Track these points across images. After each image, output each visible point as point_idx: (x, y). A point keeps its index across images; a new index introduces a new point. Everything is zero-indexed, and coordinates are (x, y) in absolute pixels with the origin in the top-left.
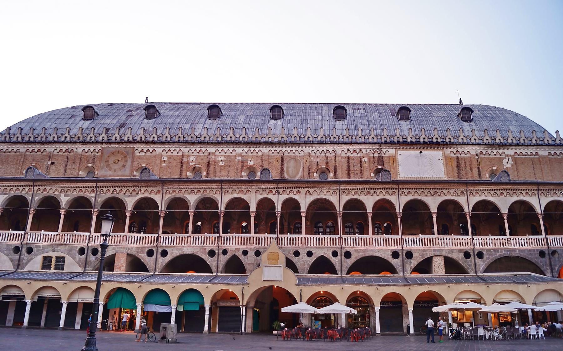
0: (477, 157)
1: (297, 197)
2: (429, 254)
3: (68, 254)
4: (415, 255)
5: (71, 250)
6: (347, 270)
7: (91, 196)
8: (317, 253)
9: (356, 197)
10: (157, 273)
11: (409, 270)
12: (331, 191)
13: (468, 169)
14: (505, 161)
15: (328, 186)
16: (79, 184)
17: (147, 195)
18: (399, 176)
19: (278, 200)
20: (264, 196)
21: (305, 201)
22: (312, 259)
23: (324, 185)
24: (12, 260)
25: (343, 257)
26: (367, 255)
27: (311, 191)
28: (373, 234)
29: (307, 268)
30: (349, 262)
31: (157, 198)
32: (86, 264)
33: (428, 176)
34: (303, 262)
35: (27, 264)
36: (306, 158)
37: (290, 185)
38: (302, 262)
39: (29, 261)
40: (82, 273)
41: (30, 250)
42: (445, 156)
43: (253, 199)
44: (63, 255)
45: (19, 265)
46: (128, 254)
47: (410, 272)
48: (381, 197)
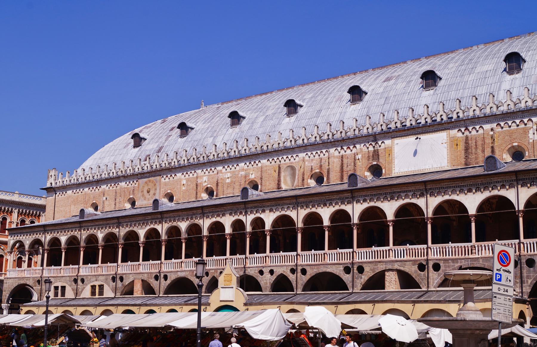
0: (492, 133)
1: (262, 216)
2: (381, 267)
3: (105, 282)
4: (367, 269)
5: (107, 279)
6: (302, 287)
7: (116, 231)
8: (278, 271)
9: (314, 210)
10: (161, 295)
11: (359, 286)
12: (291, 206)
13: (479, 151)
14: (531, 132)
15: (288, 202)
16: (108, 222)
17: (152, 226)
18: (393, 172)
19: (248, 219)
20: (236, 217)
21: (269, 218)
22: (274, 277)
23: (285, 201)
24: (73, 290)
25: (299, 274)
26: (321, 271)
27: (274, 208)
28: (329, 249)
29: (269, 285)
30: (305, 279)
31: (159, 227)
32: (115, 290)
33: (427, 167)
34: (266, 280)
35: (82, 292)
36: (301, 162)
37: (256, 205)
38: (265, 281)
39: (83, 290)
40: (112, 298)
41: (83, 281)
42: (450, 138)
43: (227, 221)
44: (102, 283)
45: (77, 294)
46: (142, 280)
47: (360, 288)
48: (337, 208)
